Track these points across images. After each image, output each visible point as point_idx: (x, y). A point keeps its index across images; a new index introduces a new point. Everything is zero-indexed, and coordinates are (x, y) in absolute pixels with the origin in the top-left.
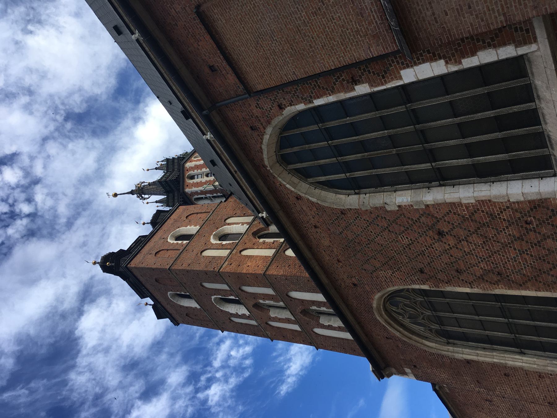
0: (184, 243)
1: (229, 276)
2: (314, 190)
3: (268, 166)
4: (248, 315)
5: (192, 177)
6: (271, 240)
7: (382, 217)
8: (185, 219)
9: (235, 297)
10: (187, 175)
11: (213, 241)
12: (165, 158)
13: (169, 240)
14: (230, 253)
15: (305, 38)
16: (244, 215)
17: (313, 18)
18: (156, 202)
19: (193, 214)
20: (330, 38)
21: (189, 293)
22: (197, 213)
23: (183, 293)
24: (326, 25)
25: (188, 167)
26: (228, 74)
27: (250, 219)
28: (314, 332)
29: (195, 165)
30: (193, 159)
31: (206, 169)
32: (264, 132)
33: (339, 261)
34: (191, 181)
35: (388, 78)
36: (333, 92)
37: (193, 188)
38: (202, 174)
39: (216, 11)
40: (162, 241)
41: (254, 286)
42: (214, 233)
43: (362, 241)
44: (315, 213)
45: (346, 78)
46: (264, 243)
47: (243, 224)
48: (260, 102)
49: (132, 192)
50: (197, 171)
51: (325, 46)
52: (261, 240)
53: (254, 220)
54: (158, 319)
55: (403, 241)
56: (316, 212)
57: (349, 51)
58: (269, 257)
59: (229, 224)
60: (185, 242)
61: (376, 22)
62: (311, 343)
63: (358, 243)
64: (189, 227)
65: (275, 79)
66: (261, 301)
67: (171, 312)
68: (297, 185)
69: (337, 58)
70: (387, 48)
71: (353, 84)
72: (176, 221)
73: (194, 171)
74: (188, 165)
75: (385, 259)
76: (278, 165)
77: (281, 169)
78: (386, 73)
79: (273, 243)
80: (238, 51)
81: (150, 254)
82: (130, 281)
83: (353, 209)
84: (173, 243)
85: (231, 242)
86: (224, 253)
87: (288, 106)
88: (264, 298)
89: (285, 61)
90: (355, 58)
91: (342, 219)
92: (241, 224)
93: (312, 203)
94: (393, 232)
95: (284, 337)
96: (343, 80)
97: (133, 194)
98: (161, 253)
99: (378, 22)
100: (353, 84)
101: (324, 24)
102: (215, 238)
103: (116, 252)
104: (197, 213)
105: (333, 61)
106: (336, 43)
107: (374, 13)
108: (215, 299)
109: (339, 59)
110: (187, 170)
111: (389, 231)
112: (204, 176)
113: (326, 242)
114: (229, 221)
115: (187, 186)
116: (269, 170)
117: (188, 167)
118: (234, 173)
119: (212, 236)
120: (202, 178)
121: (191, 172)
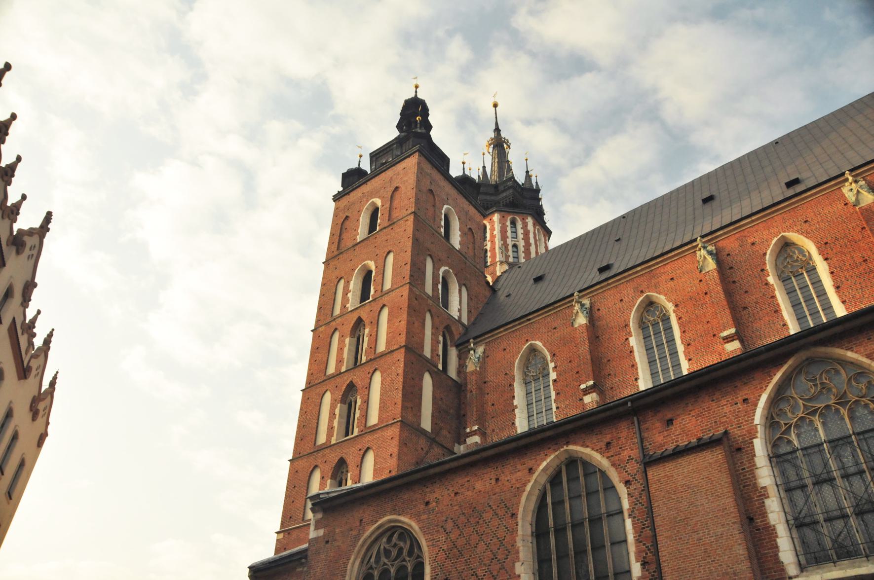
1: (402, 296)
2: (538, 489)
3: (567, 448)
4: (347, 306)
5: (513, 223)
6: (441, 353)
7: (508, 555)
8: (468, 227)
9: (372, 295)
12: (540, 188)
13: (445, 207)
14: (429, 297)
15: (687, 535)
16: (469, 312)
17: (703, 548)
18: (484, 167)
19: (474, 237)
20: (685, 559)
21: (379, 231)
22: (474, 243)
23: (379, 221)
24: (695, 558)
25: (527, 221)
26: (664, 437)
27: (465, 320)
28: (325, 392)
29: (529, 232)
30: (537, 227)
31: (523, 246)
32: (604, 456)
33: (456, 494)
34: (508, 223)
36: (638, 541)
38: (516, 238)
39: (720, 457)
40: (445, 198)
41: (389, 327)
42: (451, 271)
43: (481, 527)
44: (514, 484)
45: (649, 557)
46: (438, 342)
47: (460, 310)
48: (634, 462)
49: (497, 130)
50: (522, 233)
51: (679, 552)
52: (441, 338)
53: (463, 325)
54: (343, 174)
55: (481, 570)
56: (514, 486)
58: (423, 351)
59: (460, 291)
60: (442, 230)
62: (310, 383)
63: (478, 522)
64: (460, 233)
66: (367, 331)
67: (352, 194)
71: (642, 561)
72: (467, 213)
73: (521, 228)
74: (530, 221)
75: (460, 546)
77: (563, 459)
79: (437, 355)
80: (684, 466)
81: (431, 182)
82: (393, 144)
83: (517, 528)
85: (440, 296)
88: (371, 335)
89: (671, 510)
90: (665, 576)
91: (506, 512)
92: (459, 308)
93: (525, 485)
94: (491, 562)
96: (647, 554)
97: (495, 131)
98: (431, 196)
100: (642, 561)
101: (696, 557)
103: (429, 118)
104: (474, 243)
106: (680, 563)
110: (523, 219)
111: (493, 559)
112: (513, 242)
113: (479, 486)
114: (464, 289)
115: (503, 217)
116: (563, 447)
117: (527, 221)
118: (529, 318)
119: (447, 268)
120: (512, 238)
121: (519, 225)
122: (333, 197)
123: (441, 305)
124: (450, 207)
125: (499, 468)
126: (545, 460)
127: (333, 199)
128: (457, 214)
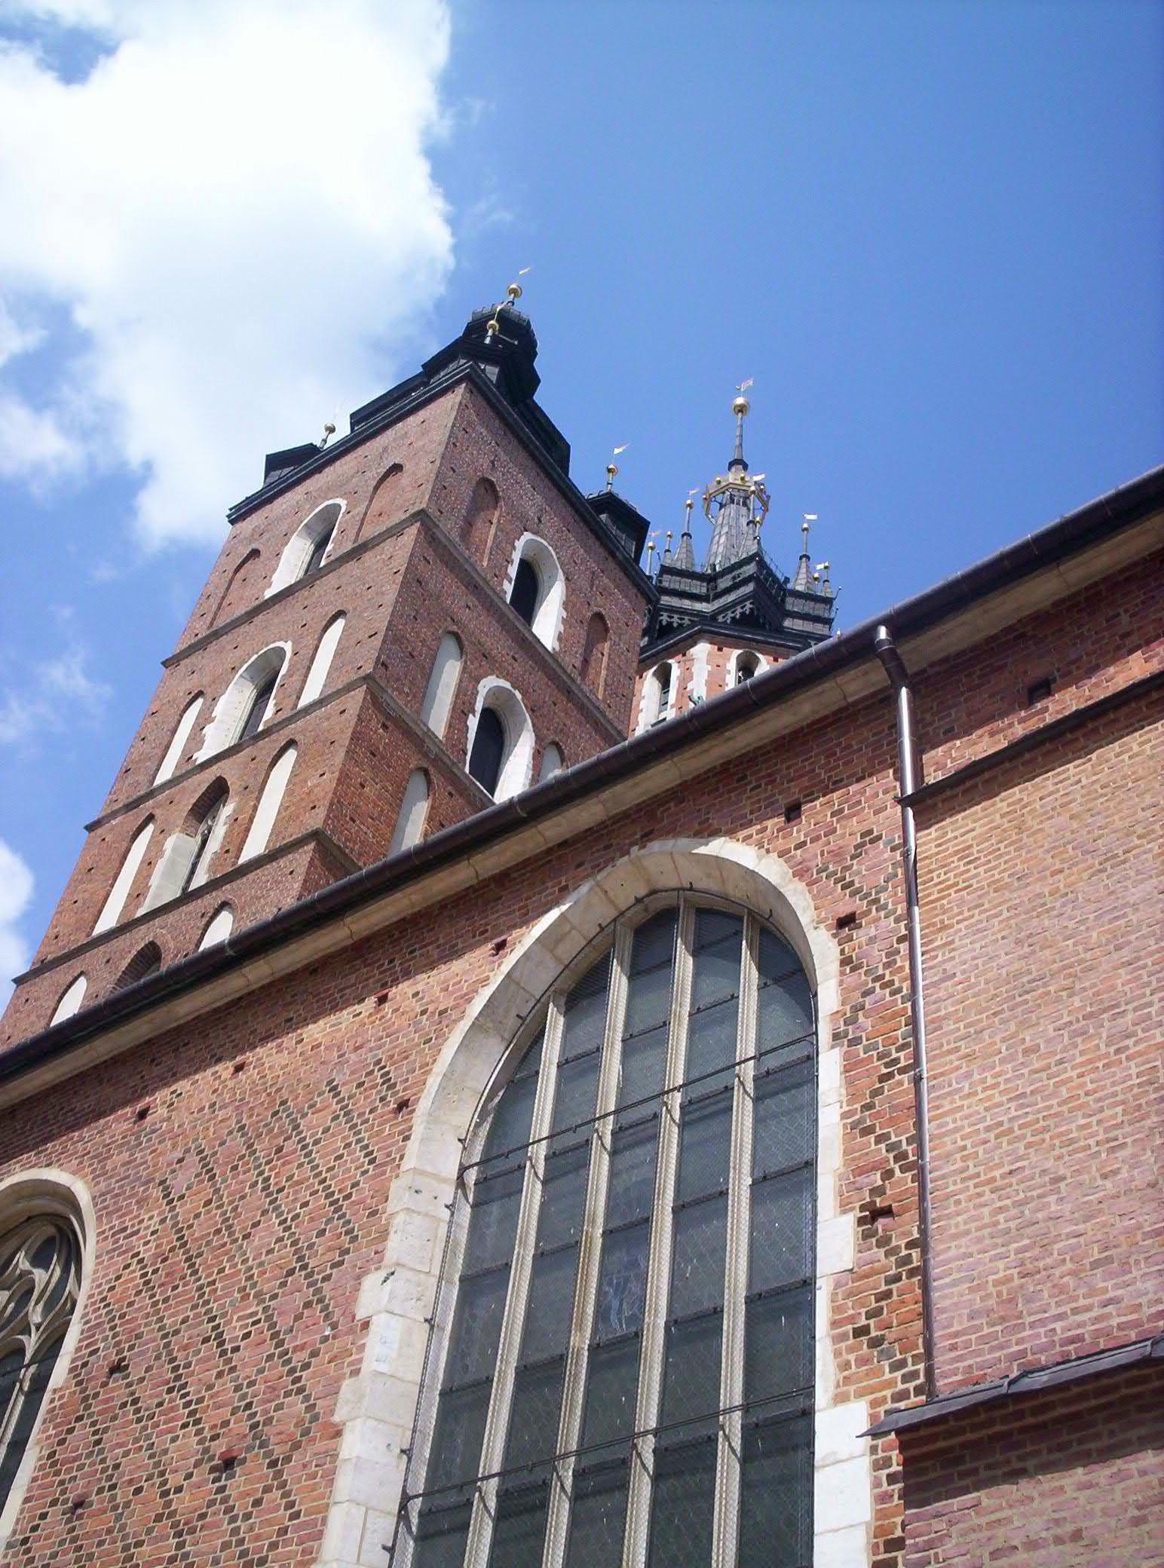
0: (506, 582)
7: (347, 1251)
10: (759, 656)
11: (489, 683)
13: (527, 536)
15: (1065, 1033)
17: (1134, 1071)
20: (1046, 1129)
24: (1094, 1119)
28: (76, 979)
32: (768, 851)
35: (851, 1350)
37: (709, 668)
42: (519, 696)
43: (284, 1164)
51: (1022, 1106)
55: (239, 1319)
56: (431, 1008)
57: (979, 1195)
60: (509, 588)
61: (1060, 1317)
63: (279, 1150)
65: (945, 902)
68: (552, 951)
69: (964, 1148)
70: (953, 1348)
75: (196, 1240)
76: (642, 891)
77: (625, 899)
78: (875, 1343)
80: (1077, 778)
83: (405, 1147)
84: (514, 548)
86: (438, 721)
87: (842, 952)
88: (236, 820)
90: (949, 1217)
91: (382, 1099)
94: (283, 1284)
95: (90, 870)
96: (888, 1174)
99: (1058, 1326)
100: (862, 1208)
101: (1101, 1110)
102: (496, 692)
105: (956, 1130)
106: (1022, 1152)
107: (1096, 1312)
108: (281, 653)
109: (958, 1156)
111: (291, 1273)
116: (628, 853)
119: (507, 685)
122: (229, 512)
123: (467, 770)
124: (546, 544)
125: (397, 962)
126: (556, 903)
127: (229, 516)
128: (562, 564)
